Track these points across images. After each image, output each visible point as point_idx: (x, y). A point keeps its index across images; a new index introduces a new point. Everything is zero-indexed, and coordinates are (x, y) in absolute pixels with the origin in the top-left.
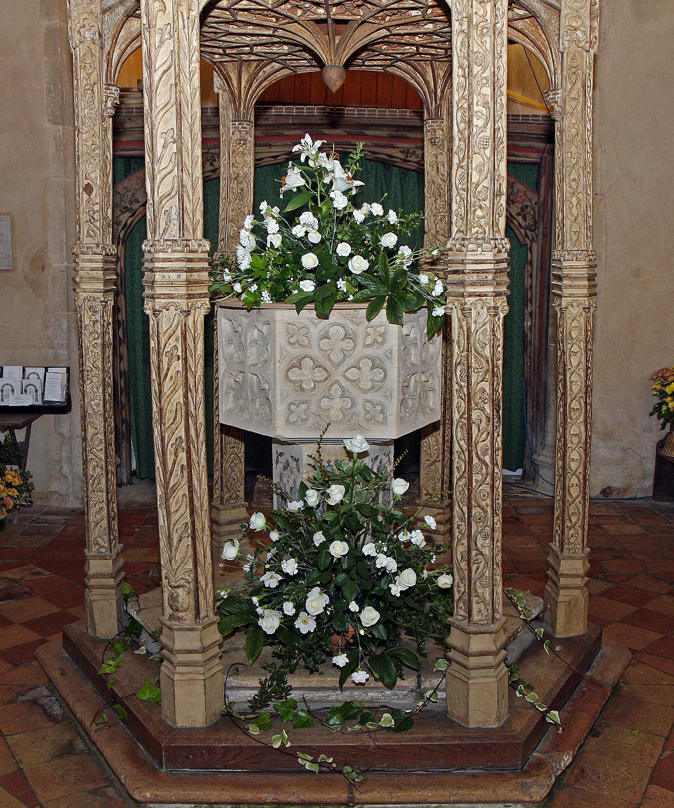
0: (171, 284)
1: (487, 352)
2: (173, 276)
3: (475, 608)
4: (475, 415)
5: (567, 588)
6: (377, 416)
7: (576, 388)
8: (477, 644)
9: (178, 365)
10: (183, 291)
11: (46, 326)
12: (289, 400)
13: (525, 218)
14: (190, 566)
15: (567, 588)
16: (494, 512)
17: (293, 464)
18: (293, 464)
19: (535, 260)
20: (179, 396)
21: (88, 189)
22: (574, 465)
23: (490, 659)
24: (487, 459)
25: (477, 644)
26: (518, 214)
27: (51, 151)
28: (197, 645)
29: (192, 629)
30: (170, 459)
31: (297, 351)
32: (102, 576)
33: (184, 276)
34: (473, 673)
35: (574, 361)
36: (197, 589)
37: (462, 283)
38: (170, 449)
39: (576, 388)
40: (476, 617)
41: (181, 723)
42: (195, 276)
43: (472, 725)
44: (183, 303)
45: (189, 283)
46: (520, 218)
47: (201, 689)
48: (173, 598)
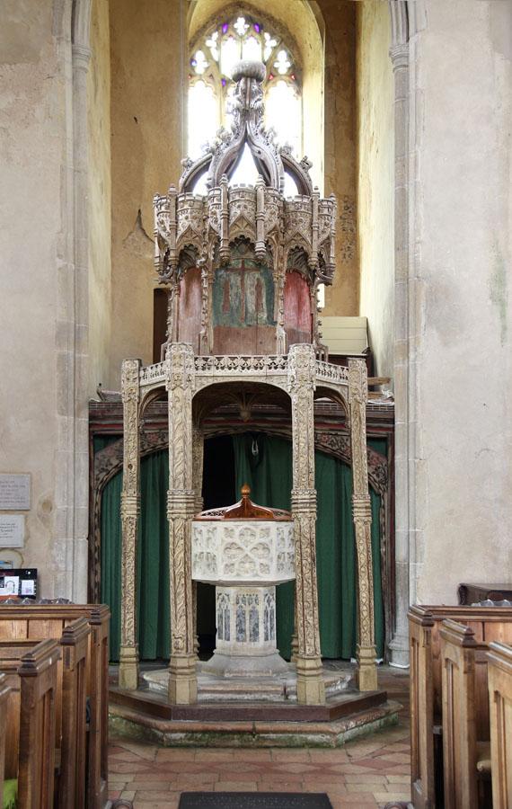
0: (180, 508)
1: (308, 536)
2: (181, 505)
3: (307, 648)
4: (304, 562)
5: (364, 664)
6: (265, 568)
7: (363, 561)
8: (309, 664)
9: (182, 542)
10: (184, 511)
11: (51, 548)
12: (225, 563)
13: (378, 476)
14: (185, 628)
15: (364, 664)
16: (314, 604)
17: (226, 597)
18: (226, 597)
19: (386, 505)
20: (182, 554)
21: (130, 466)
22: (364, 600)
23: (314, 672)
24: (310, 581)
25: (309, 664)
26: (373, 473)
27: (59, 432)
28: (186, 665)
29: (184, 657)
30: (177, 581)
31: (229, 540)
32: (131, 657)
33: (185, 505)
34: (308, 678)
35: (361, 548)
36: (187, 639)
37: (297, 508)
38: (178, 578)
39: (363, 561)
40: (307, 652)
41: (179, 702)
42: (189, 505)
43: (308, 704)
44: (185, 516)
45: (187, 508)
46: (374, 476)
47: (187, 685)
48: (177, 643)
